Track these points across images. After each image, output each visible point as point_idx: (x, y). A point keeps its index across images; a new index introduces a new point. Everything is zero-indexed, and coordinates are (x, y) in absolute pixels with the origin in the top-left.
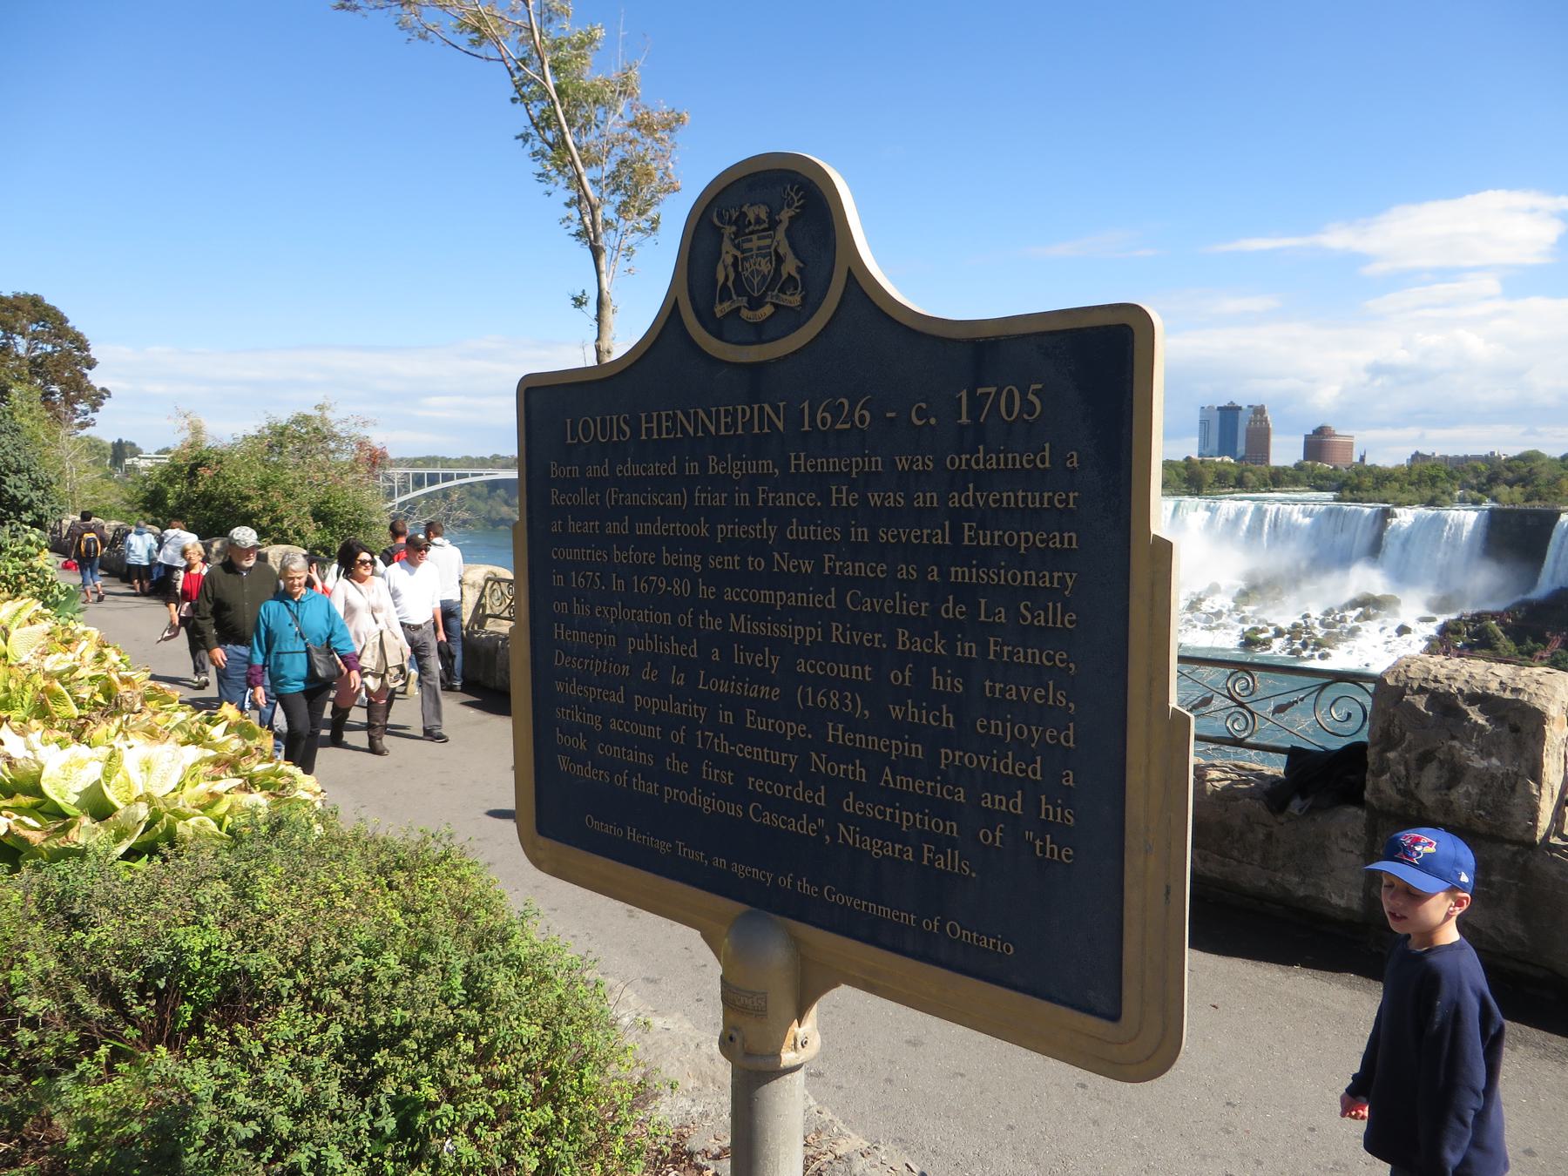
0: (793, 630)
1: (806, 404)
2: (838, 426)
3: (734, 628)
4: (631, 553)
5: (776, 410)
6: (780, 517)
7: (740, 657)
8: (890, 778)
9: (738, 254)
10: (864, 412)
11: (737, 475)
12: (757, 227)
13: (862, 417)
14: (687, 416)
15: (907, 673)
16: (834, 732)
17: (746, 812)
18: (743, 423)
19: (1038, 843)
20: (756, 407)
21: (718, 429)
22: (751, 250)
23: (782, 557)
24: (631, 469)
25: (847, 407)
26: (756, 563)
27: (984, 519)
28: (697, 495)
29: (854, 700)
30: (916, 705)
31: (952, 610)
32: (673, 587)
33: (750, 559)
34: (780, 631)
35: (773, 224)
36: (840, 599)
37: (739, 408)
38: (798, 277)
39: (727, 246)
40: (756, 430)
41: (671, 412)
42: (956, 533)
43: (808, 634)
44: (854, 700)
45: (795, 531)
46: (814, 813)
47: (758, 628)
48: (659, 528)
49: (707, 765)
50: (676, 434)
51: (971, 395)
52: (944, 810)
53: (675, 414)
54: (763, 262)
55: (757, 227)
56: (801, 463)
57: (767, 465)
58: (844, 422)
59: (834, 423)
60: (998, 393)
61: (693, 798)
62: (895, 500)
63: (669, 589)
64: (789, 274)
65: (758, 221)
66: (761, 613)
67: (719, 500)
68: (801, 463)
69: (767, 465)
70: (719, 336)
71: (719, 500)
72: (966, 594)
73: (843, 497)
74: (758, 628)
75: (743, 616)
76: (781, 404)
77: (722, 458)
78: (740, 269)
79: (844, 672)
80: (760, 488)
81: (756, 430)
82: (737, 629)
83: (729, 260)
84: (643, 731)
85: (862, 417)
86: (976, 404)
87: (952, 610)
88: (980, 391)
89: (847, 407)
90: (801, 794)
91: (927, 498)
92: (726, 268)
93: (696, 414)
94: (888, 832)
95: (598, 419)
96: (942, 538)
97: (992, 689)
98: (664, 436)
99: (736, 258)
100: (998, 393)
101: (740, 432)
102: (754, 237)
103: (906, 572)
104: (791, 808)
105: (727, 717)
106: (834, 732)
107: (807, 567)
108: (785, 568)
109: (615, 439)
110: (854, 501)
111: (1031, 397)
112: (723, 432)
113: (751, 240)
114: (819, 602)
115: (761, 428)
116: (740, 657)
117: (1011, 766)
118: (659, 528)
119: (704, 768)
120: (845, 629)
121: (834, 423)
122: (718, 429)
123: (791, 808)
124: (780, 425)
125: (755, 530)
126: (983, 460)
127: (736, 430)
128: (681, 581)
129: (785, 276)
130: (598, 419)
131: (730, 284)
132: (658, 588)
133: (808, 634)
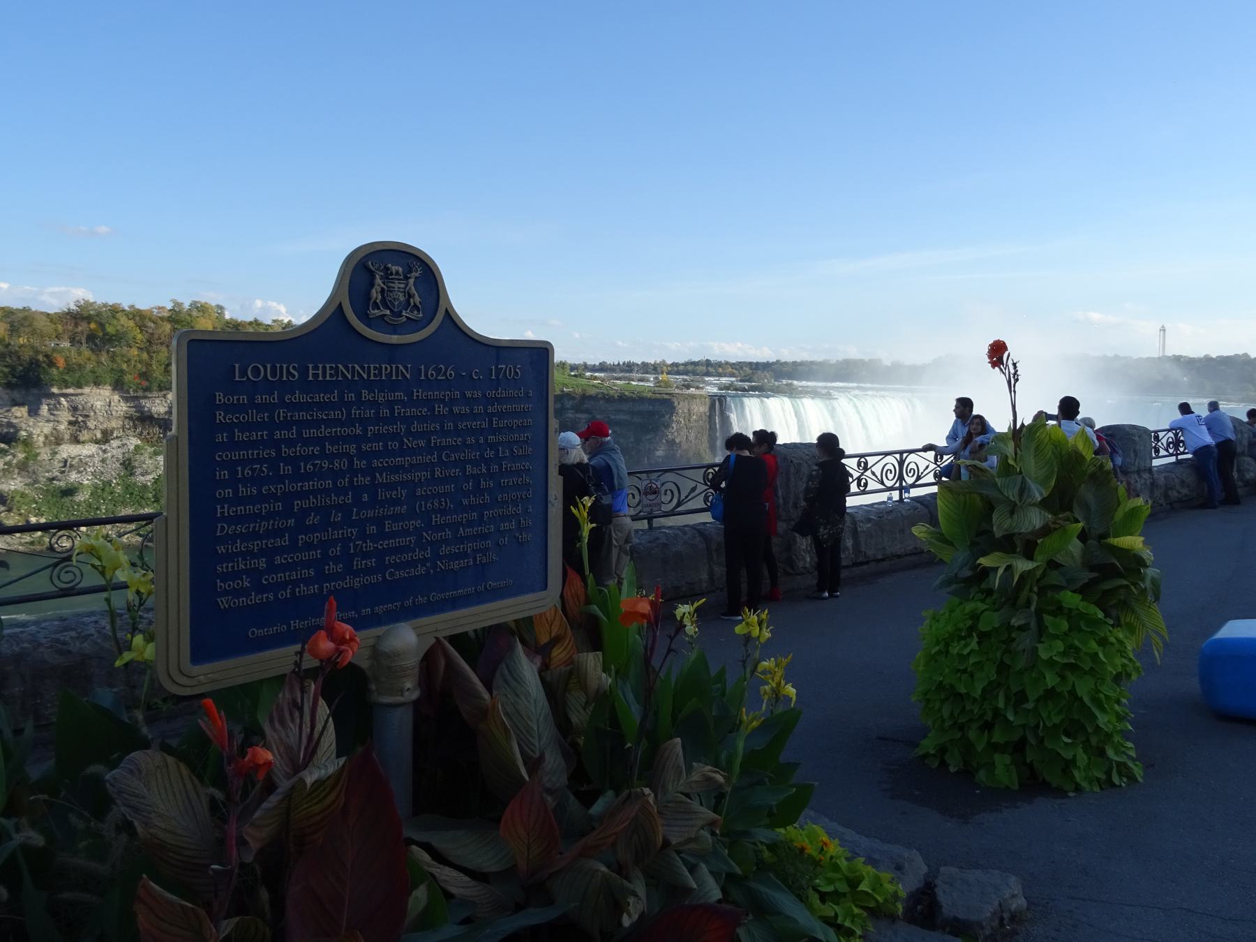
0: (415, 475)
1: (423, 367)
2: (439, 378)
3: (378, 481)
4: (298, 449)
5: (406, 368)
6: (407, 420)
7: (382, 495)
8: (462, 532)
9: (385, 287)
10: (452, 372)
11: (381, 401)
12: (397, 277)
13: (451, 374)
14: (347, 368)
15: (470, 484)
16: (437, 519)
17: (384, 577)
18: (385, 374)
19: (520, 537)
20: (394, 366)
21: (369, 375)
22: (394, 288)
23: (409, 440)
24: (298, 397)
25: (443, 370)
26: (394, 445)
27: (501, 415)
28: (353, 411)
29: (446, 502)
30: (475, 496)
31: (489, 453)
32: (334, 465)
33: (390, 443)
34: (406, 477)
35: (406, 278)
36: (440, 457)
37: (383, 366)
38: (420, 306)
39: (378, 281)
40: (394, 378)
41: (378, 366)
42: (491, 423)
43: (423, 475)
44: (446, 502)
45: (416, 427)
46: (423, 561)
47: (395, 478)
48: (324, 431)
49: (358, 561)
50: (338, 377)
51: (497, 367)
52: (484, 537)
53: (337, 367)
54: (401, 295)
55: (397, 277)
56: (418, 393)
57: (400, 395)
58: (443, 376)
59: (437, 375)
60: (506, 368)
61: (348, 582)
62: (465, 410)
63: (331, 466)
64: (414, 303)
65: (397, 273)
66: (397, 469)
67: (369, 413)
68: (418, 393)
69: (400, 395)
70: (369, 326)
71: (369, 413)
72: (493, 446)
73: (441, 409)
74: (395, 478)
75: (384, 474)
76: (409, 366)
77: (371, 391)
78: (386, 295)
79: (441, 489)
80: (396, 407)
81: (394, 378)
82: (381, 481)
83: (379, 289)
84: (305, 556)
85: (451, 374)
86: (498, 371)
87: (489, 453)
88: (500, 366)
89: (443, 370)
90: (418, 554)
91: (478, 409)
92: (377, 293)
93: (353, 367)
94: (464, 555)
95: (269, 366)
96: (485, 425)
97: (504, 482)
98: (328, 378)
99: (383, 289)
100: (506, 368)
101: (384, 378)
102: (396, 282)
103: (470, 440)
104: (412, 564)
105: (373, 529)
106: (437, 519)
107: (422, 443)
108: (410, 446)
109: (285, 379)
110: (446, 411)
111: (517, 370)
112: (372, 378)
113: (394, 283)
114: (429, 460)
115: (397, 376)
116: (382, 495)
117: (511, 510)
118: (324, 431)
119: (355, 563)
120: (441, 469)
121: (437, 375)
122: (369, 375)
123: (412, 564)
124: (408, 376)
125: (393, 429)
126: (501, 393)
127: (381, 377)
128: (341, 461)
129: (412, 304)
130: (269, 366)
131: (378, 301)
132: (321, 467)
133: (423, 475)
